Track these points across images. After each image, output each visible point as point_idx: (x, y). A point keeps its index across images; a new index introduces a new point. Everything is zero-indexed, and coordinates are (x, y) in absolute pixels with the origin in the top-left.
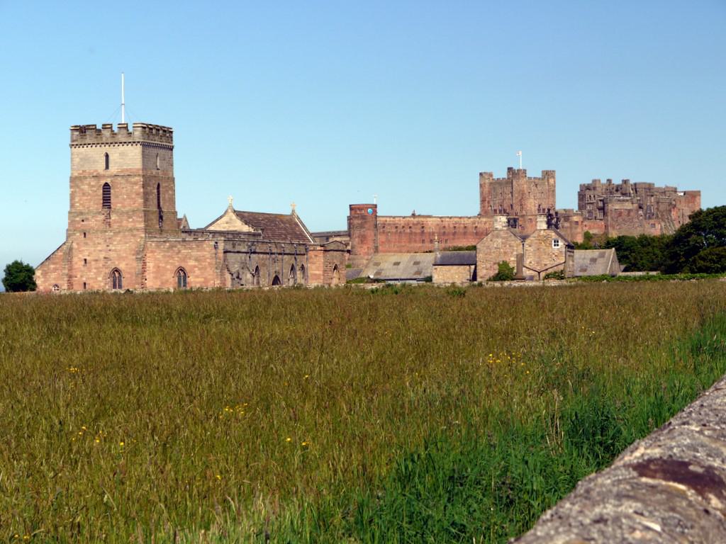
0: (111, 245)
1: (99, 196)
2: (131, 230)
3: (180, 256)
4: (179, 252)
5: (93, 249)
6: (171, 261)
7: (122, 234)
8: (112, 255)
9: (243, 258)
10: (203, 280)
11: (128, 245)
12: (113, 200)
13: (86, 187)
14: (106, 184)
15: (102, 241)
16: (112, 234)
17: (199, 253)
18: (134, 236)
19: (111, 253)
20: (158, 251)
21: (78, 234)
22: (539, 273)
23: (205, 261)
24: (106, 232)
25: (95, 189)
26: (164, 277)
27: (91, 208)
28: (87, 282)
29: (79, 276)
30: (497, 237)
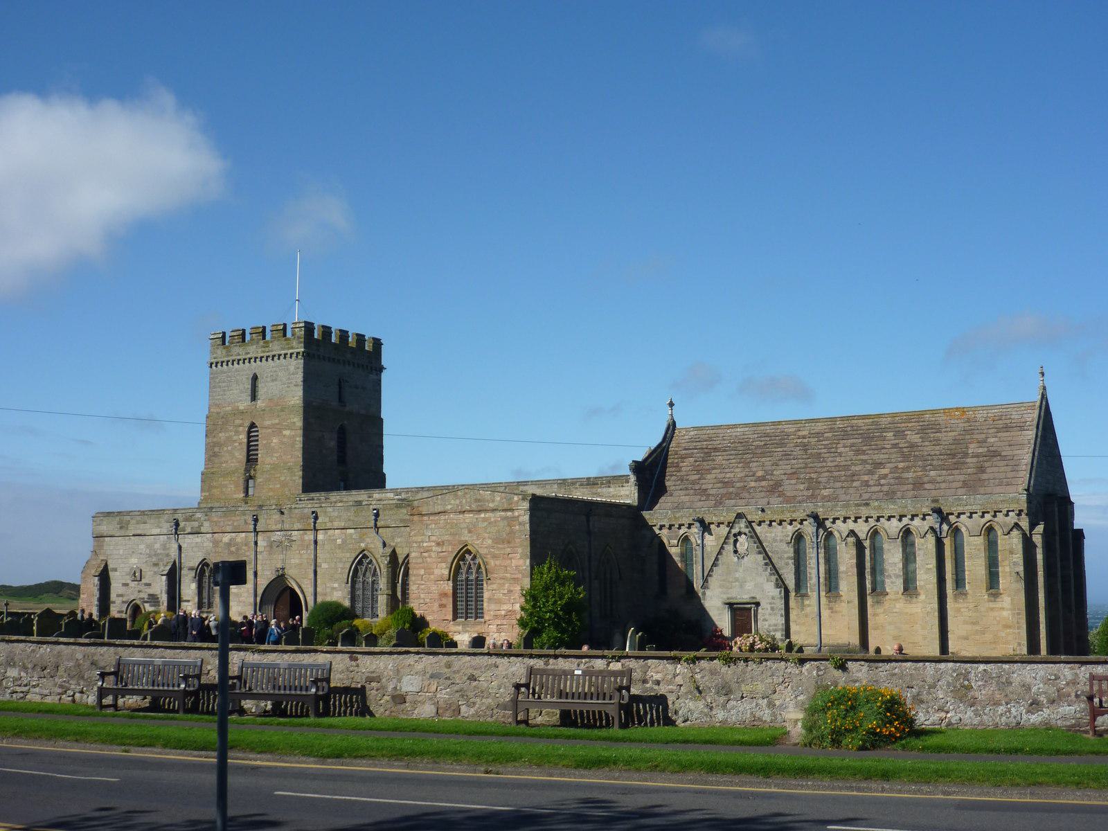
9: (157, 546)
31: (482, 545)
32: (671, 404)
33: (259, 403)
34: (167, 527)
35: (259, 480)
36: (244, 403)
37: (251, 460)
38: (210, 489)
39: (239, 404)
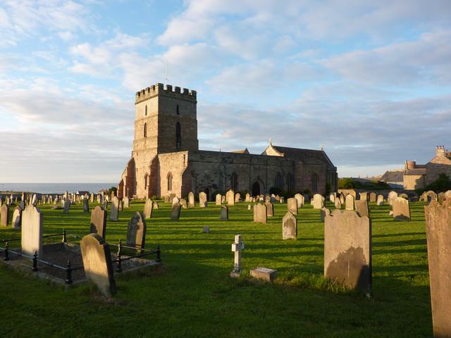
9: (216, 166)
31: (317, 172)
33: (180, 116)
34: (220, 160)
35: (183, 143)
36: (174, 114)
37: (178, 135)
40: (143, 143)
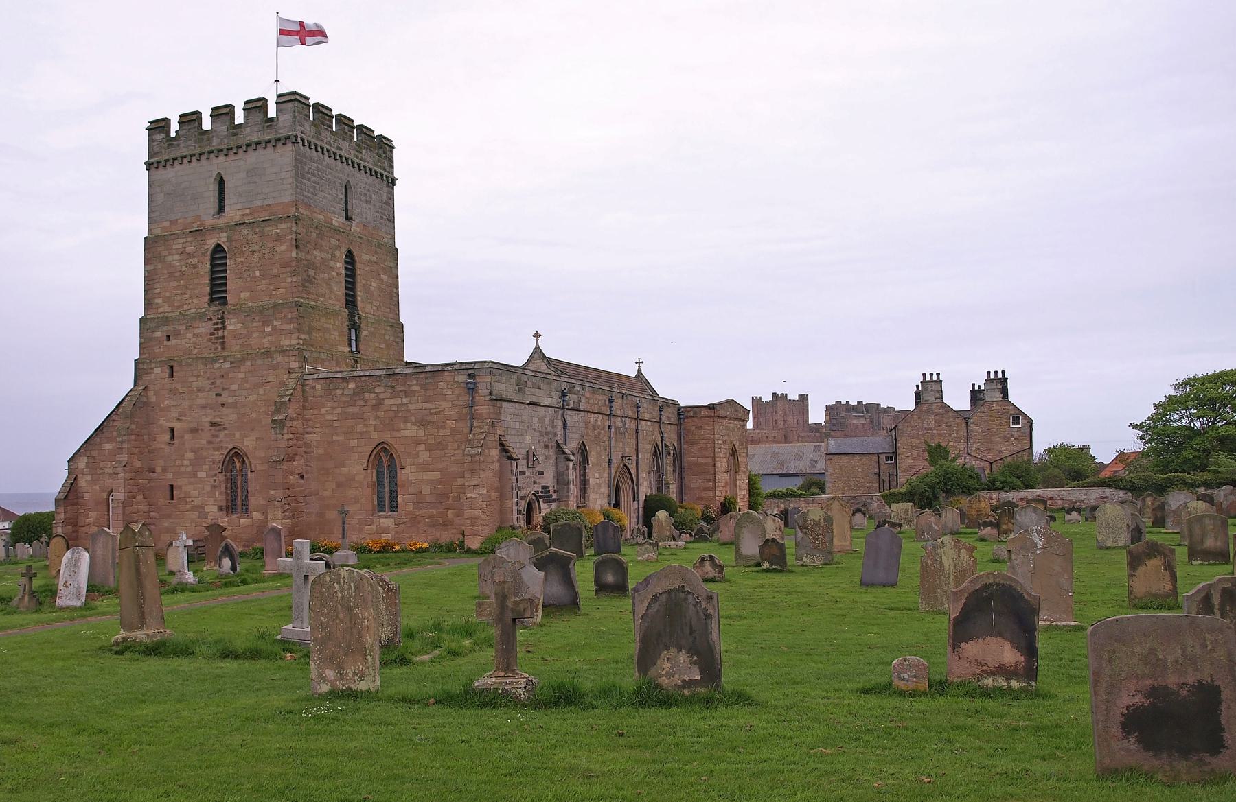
0: (225, 394)
1: (202, 276)
2: (268, 354)
3: (381, 413)
4: (380, 403)
5: (187, 403)
6: (359, 428)
7: (249, 363)
8: (228, 416)
9: (547, 421)
10: (436, 475)
11: (261, 391)
12: (231, 285)
13: (177, 257)
14: (218, 248)
15: (204, 384)
16: (227, 365)
17: (426, 405)
18: (275, 367)
19: (225, 411)
20: (329, 404)
21: (158, 370)
22: (991, 463)
23: (444, 427)
24: (215, 360)
25: (193, 261)
26: (345, 470)
27: (186, 307)
28: (174, 484)
29: (159, 469)
30: (928, 413)
32: (537, 336)
36: (338, 220)
38: (310, 330)
39: (333, 216)
40: (205, 328)
